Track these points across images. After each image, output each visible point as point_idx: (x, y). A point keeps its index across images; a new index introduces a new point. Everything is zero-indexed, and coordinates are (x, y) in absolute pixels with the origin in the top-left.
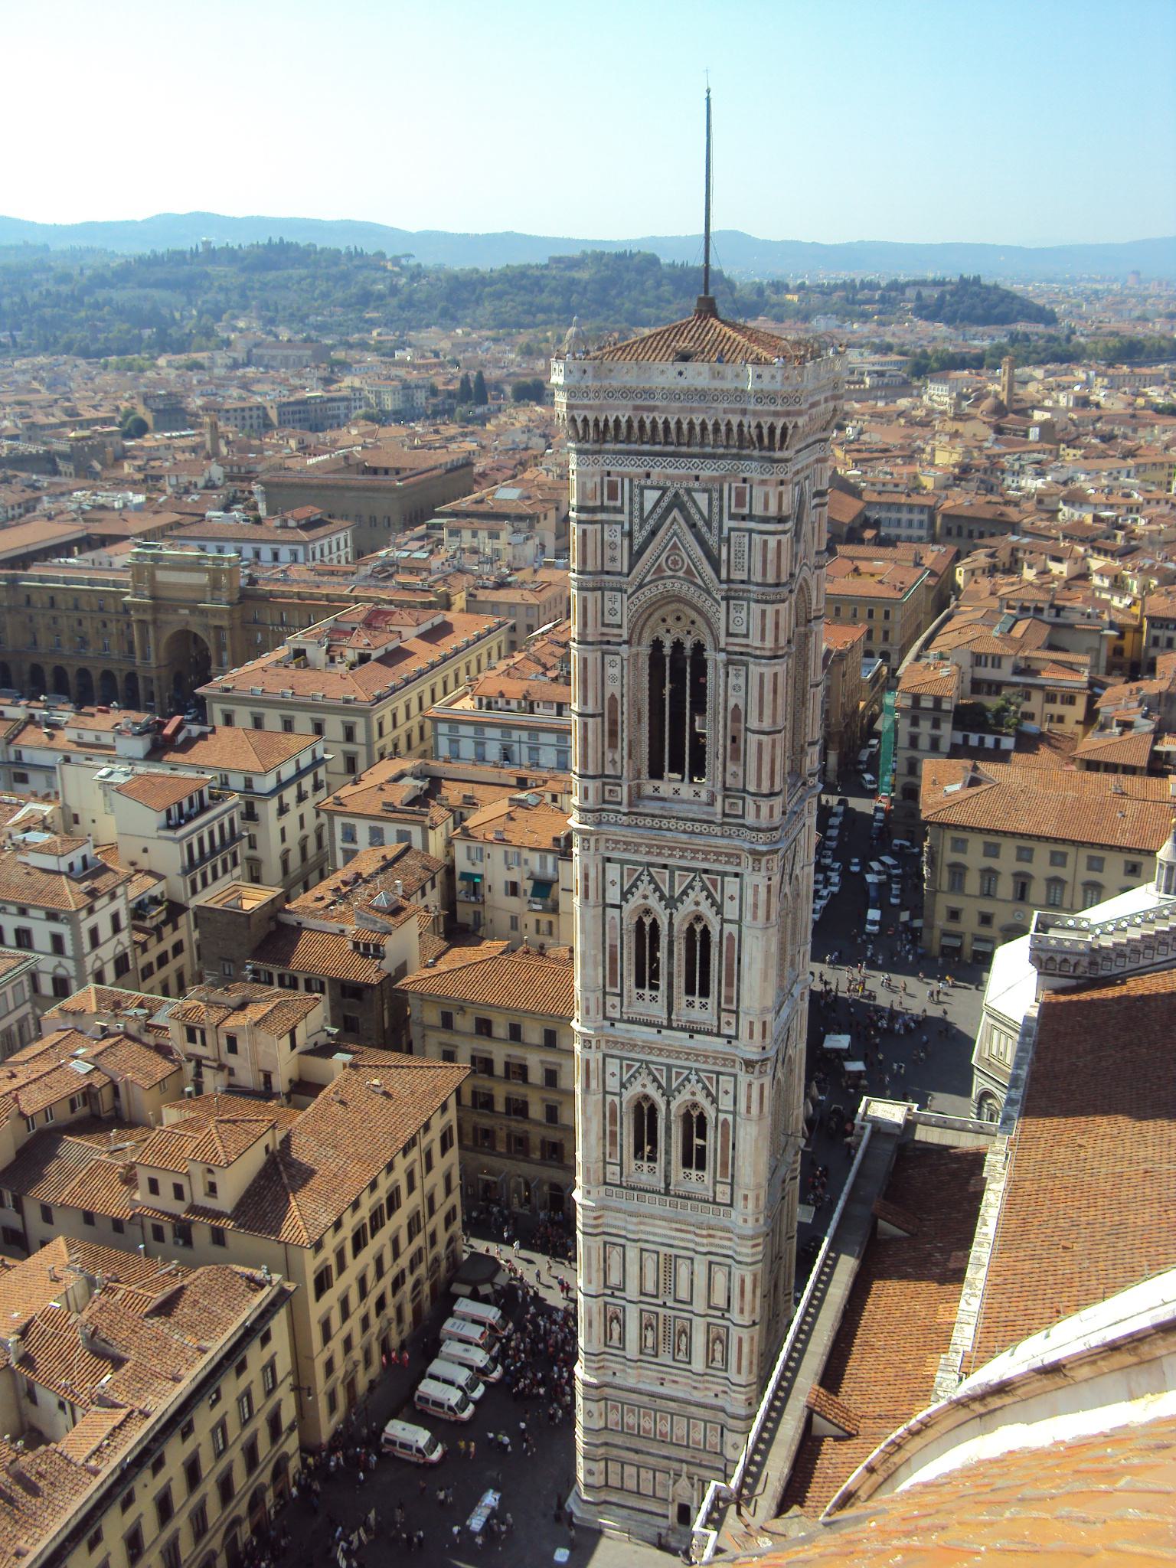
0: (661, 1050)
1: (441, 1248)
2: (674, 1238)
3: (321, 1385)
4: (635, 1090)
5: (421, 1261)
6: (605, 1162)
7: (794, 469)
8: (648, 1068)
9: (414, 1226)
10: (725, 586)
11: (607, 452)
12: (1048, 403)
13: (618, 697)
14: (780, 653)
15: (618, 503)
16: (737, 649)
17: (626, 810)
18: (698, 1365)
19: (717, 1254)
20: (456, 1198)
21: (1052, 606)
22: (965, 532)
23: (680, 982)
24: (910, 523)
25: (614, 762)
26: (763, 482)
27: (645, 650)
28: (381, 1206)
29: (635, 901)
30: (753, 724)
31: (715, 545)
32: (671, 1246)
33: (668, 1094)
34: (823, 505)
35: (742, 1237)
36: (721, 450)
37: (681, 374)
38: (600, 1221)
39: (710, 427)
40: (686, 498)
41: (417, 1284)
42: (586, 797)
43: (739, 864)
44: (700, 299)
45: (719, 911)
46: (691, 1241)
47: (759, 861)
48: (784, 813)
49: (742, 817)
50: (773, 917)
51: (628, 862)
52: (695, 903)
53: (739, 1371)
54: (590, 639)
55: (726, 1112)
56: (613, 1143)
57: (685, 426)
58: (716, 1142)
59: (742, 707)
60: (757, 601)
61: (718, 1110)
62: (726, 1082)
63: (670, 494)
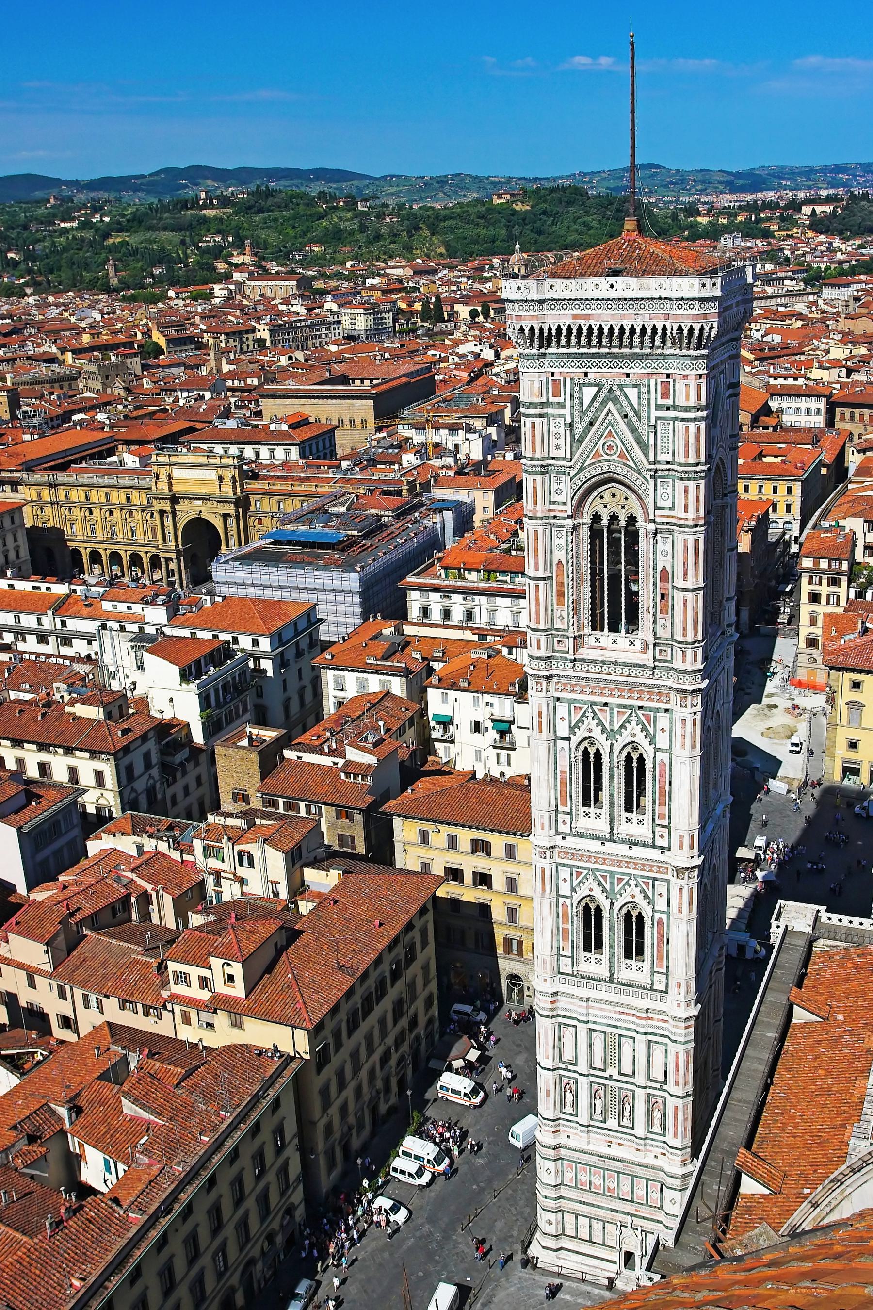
0: (605, 859)
1: (421, 1029)
2: (618, 1020)
3: (321, 1146)
4: (583, 891)
5: (403, 1040)
6: (558, 954)
8: (593, 874)
9: (398, 1010)
10: (653, 467)
13: (565, 563)
15: (561, 400)
18: (640, 1131)
19: (655, 1034)
20: (433, 986)
24: (808, 410)
25: (561, 618)
26: (685, 376)
27: (586, 520)
28: (371, 993)
29: (581, 734)
30: (679, 583)
32: (616, 1027)
33: (610, 895)
35: (675, 1019)
37: (612, 286)
38: (554, 1006)
40: (618, 393)
41: (402, 1059)
42: (539, 648)
46: (633, 1023)
51: (575, 701)
53: (675, 1135)
54: (539, 515)
55: (661, 912)
56: (565, 938)
58: (652, 938)
59: (669, 569)
60: (681, 479)
61: (654, 911)
62: (660, 887)
63: (605, 390)
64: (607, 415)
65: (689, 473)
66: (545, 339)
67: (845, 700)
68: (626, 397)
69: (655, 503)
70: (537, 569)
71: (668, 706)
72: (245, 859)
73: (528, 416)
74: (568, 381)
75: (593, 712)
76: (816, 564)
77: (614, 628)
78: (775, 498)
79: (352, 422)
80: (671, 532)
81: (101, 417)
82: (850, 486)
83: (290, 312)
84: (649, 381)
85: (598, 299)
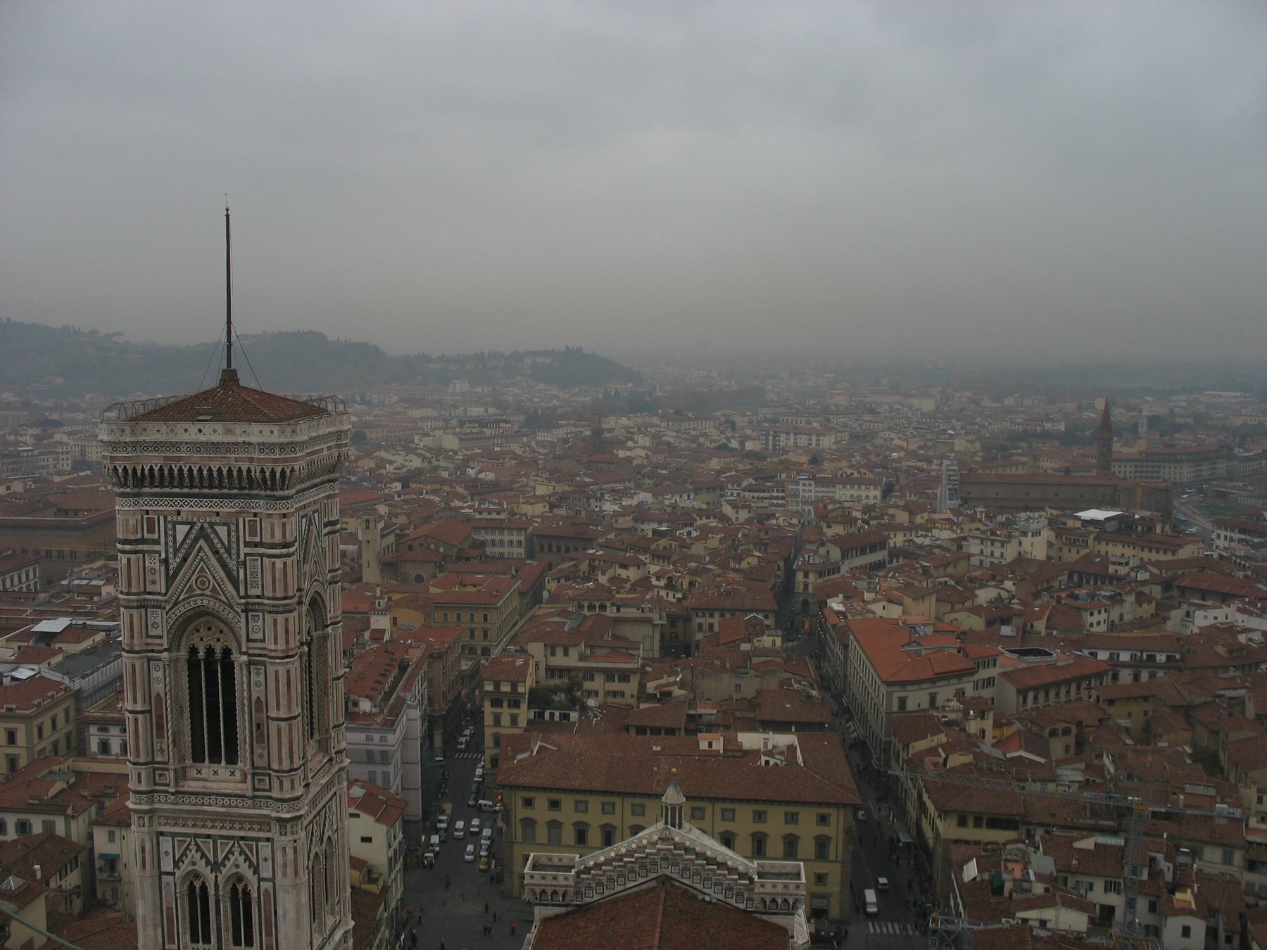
7: (299, 505)
10: (243, 601)
11: (146, 495)
12: (630, 444)
13: (162, 695)
14: (291, 653)
15: (156, 536)
16: (257, 652)
17: (173, 790)
21: (613, 605)
22: (555, 549)
23: (228, 935)
24: (511, 543)
25: (162, 750)
27: (183, 654)
29: (185, 867)
30: (273, 714)
34: (334, 532)
36: (236, 491)
37: (200, 431)
39: (225, 473)
40: (209, 531)
42: (140, 781)
43: (269, 831)
44: (224, 371)
45: (256, 871)
47: (286, 827)
49: (270, 790)
50: (301, 872)
52: (237, 864)
54: (137, 648)
57: (205, 472)
59: (263, 699)
60: (270, 612)
64: (199, 551)
70: (135, 702)
71: (269, 835)
73: (124, 552)
74: (162, 518)
75: (196, 844)
76: (497, 685)
80: (264, 664)
83: (18, 443)
85: (187, 443)
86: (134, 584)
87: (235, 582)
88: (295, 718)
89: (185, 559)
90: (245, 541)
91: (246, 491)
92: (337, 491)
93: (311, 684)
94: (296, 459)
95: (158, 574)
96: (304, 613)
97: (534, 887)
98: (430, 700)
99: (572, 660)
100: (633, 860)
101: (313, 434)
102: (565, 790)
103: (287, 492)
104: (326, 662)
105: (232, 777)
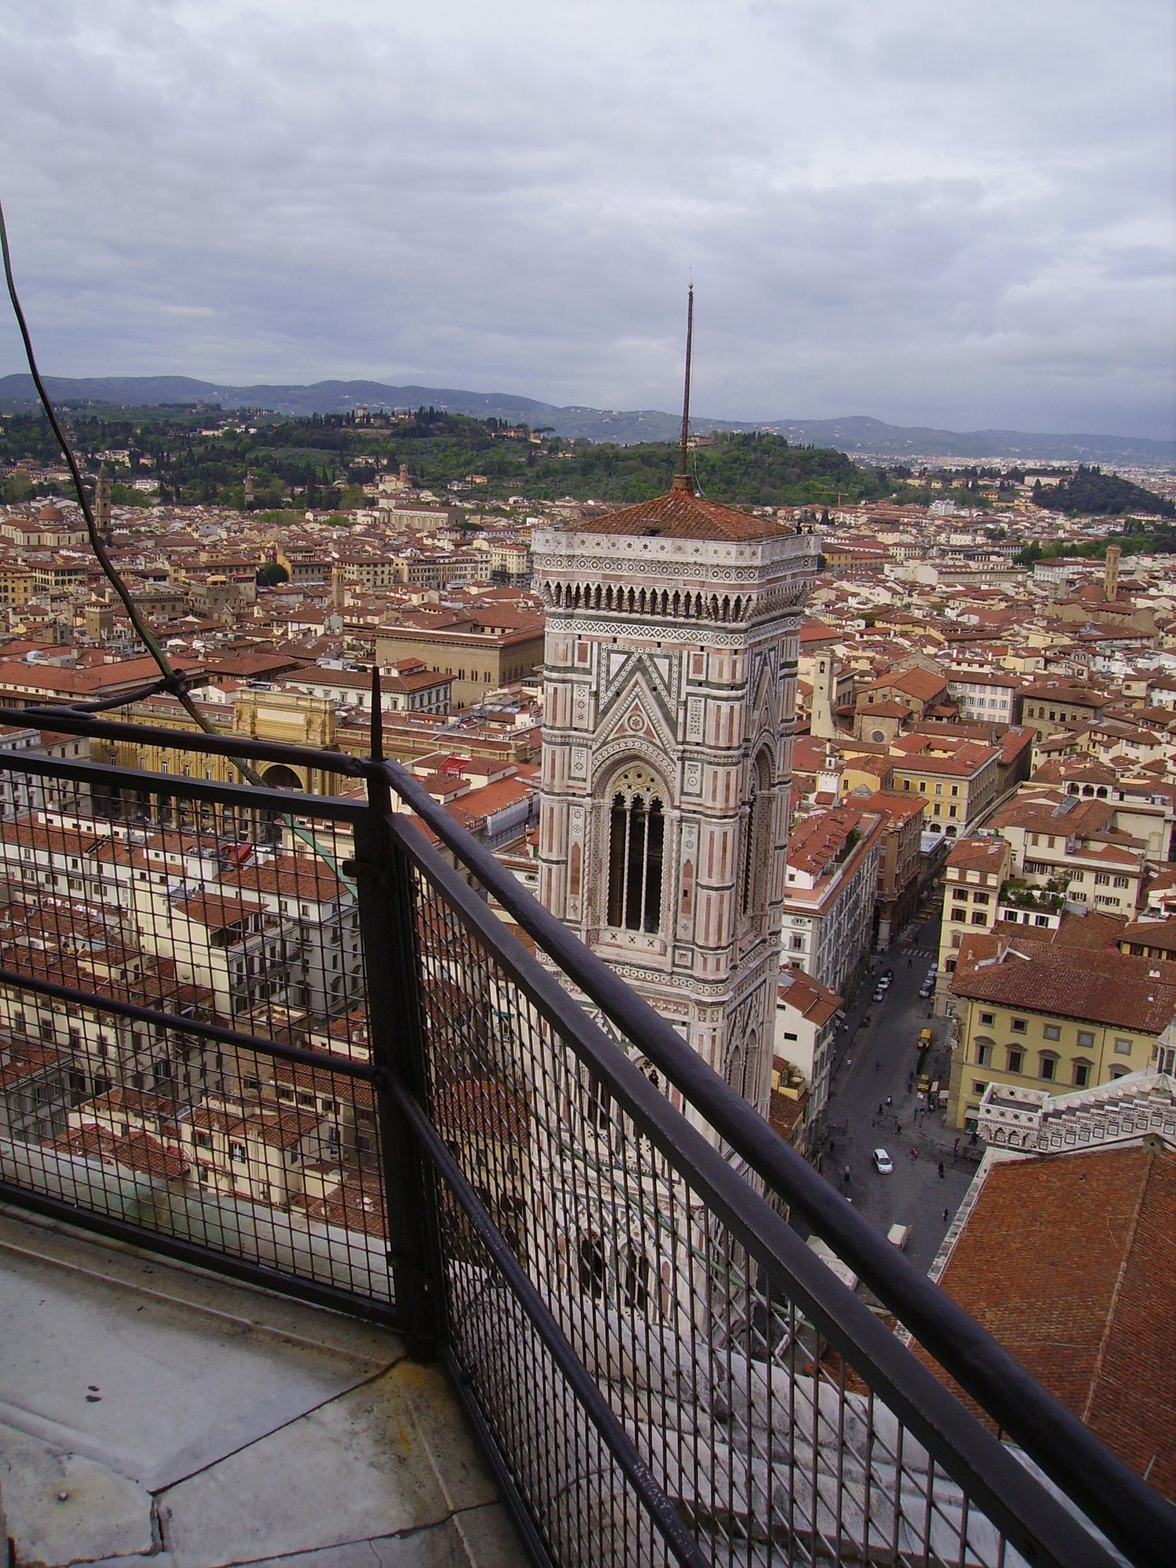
7: (750, 642)
10: (681, 747)
11: (579, 616)
13: (581, 846)
14: (731, 813)
15: (587, 665)
22: (1047, 715)
25: (575, 908)
27: (607, 802)
30: (704, 881)
31: (674, 709)
36: (682, 620)
39: (671, 597)
40: (648, 663)
48: (734, 967)
54: (556, 791)
57: (648, 596)
59: (693, 863)
60: (710, 763)
63: (634, 659)
64: (635, 686)
65: (720, 757)
66: (573, 598)
67: (974, 1034)
68: (656, 668)
69: (682, 788)
70: (550, 850)
72: (237, 1152)
73: (550, 680)
76: (963, 875)
77: (633, 924)
78: (939, 799)
79: (474, 676)
80: (698, 822)
81: (197, 644)
82: (1020, 792)
84: (681, 652)
86: (559, 717)
87: (672, 724)
88: (729, 888)
89: (618, 694)
90: (688, 679)
91: (693, 620)
92: (799, 627)
93: (749, 850)
94: (752, 586)
95: (586, 708)
96: (750, 768)
97: (989, 1124)
98: (880, 882)
99: (1058, 852)
100: (1117, 1109)
101: (776, 558)
102: (1034, 1010)
103: (742, 625)
104: (768, 826)
105: (650, 947)
